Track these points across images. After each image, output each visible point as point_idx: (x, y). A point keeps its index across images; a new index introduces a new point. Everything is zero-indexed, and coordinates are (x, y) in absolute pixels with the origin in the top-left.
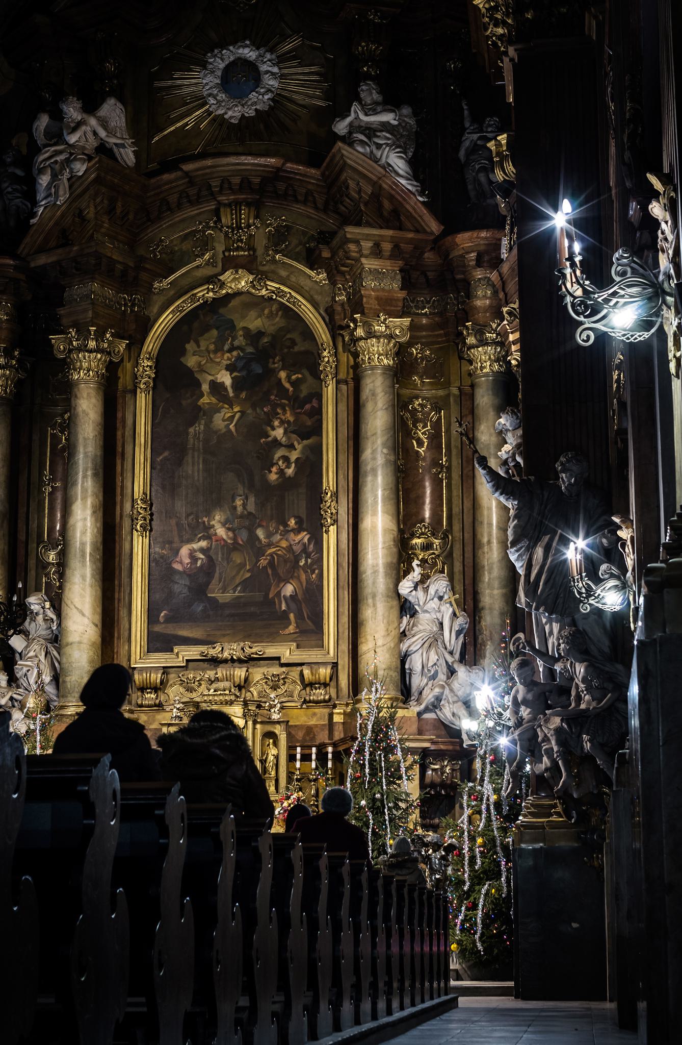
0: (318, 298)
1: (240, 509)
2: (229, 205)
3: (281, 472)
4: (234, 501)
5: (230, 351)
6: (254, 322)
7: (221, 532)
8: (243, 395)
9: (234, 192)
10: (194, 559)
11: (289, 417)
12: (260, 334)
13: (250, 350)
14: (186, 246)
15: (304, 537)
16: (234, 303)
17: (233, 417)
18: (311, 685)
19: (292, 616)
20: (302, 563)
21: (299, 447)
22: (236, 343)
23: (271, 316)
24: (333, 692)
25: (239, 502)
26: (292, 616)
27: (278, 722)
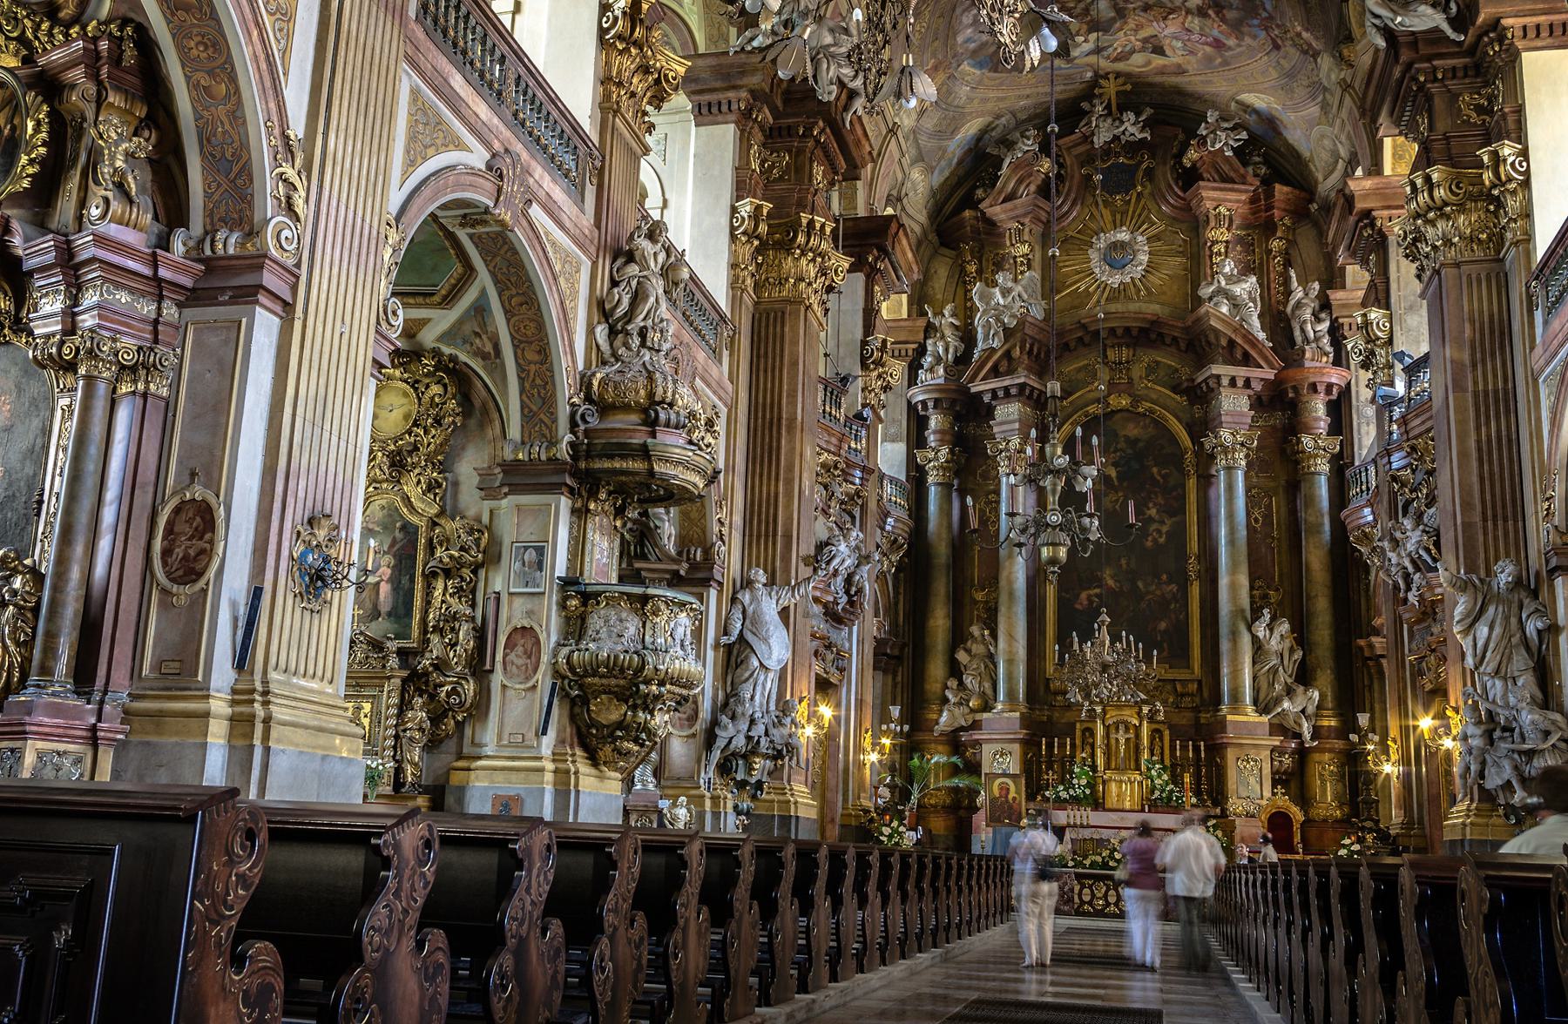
0: (1181, 414)
1: (1124, 566)
2: (1113, 347)
3: (1155, 540)
4: (1119, 558)
5: (1114, 452)
6: (1132, 430)
7: (1111, 582)
8: (1125, 484)
9: (1117, 337)
10: (1091, 602)
11: (1160, 500)
12: (1137, 440)
13: (1129, 451)
14: (1081, 376)
15: (1174, 587)
16: (1119, 416)
17: (1117, 501)
18: (1182, 695)
19: (1165, 645)
20: (1173, 606)
21: (1168, 522)
22: (1119, 446)
23: (1145, 427)
24: (1197, 700)
25: (1123, 562)
26: (1165, 645)
27: (1162, 722)
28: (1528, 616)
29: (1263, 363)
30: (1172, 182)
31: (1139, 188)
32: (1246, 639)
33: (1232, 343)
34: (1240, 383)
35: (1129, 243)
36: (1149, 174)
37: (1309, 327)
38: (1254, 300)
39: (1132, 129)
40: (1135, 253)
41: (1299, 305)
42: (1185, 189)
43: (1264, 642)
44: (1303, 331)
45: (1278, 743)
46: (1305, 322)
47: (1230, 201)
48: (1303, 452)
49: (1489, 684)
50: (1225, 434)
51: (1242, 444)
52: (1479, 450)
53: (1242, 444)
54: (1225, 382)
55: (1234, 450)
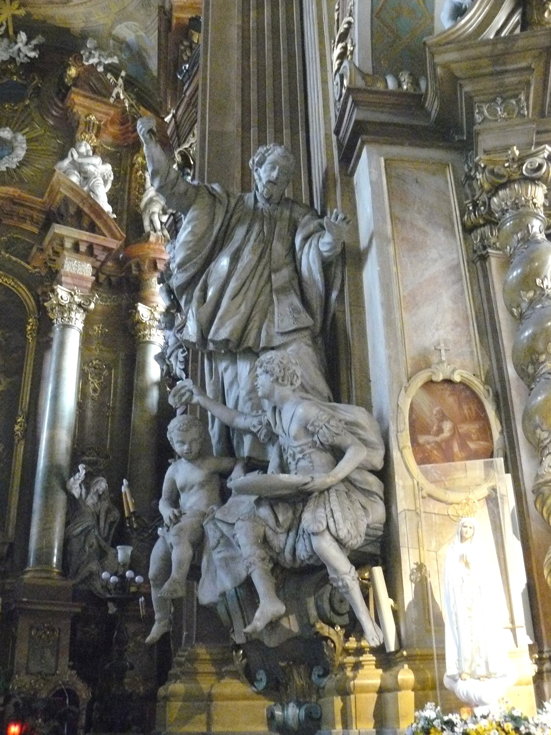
28: (306, 239)
29: (106, 233)
30: (54, 95)
31: (27, 102)
32: (61, 498)
33: (79, 213)
34: (83, 248)
35: (11, 142)
36: (37, 91)
37: (156, 218)
38: (105, 182)
39: (24, 50)
40: (13, 149)
41: (151, 201)
42: (62, 100)
43: (81, 503)
44: (152, 222)
45: (78, 610)
46: (153, 213)
47: (100, 112)
48: (139, 322)
49: (227, 378)
50: (62, 292)
51: (80, 305)
52: (245, 37)
53: (80, 305)
54: (68, 244)
55: (70, 310)
